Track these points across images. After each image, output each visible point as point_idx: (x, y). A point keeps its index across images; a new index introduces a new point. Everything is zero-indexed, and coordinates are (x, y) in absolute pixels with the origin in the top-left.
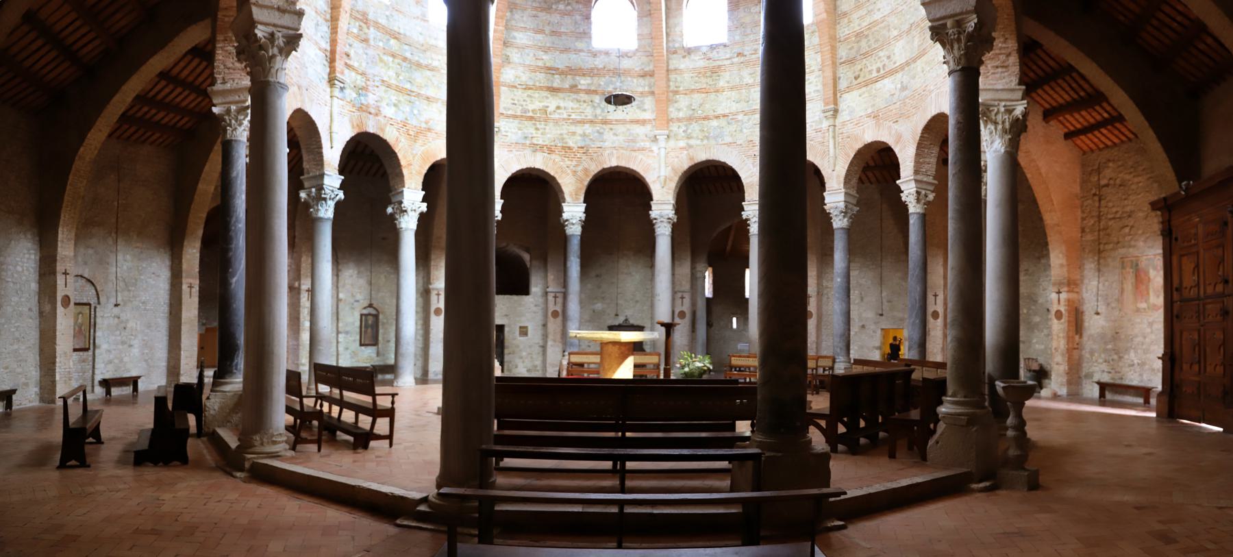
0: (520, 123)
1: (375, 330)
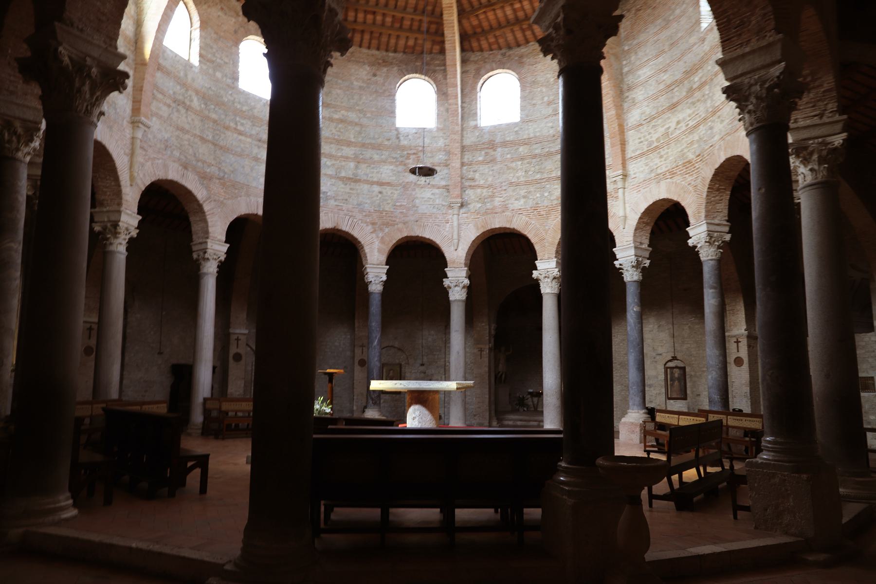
0: (646, 159)
1: (683, 384)
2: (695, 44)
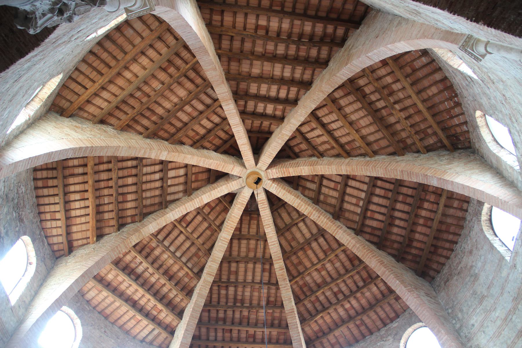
2: (509, 274)
